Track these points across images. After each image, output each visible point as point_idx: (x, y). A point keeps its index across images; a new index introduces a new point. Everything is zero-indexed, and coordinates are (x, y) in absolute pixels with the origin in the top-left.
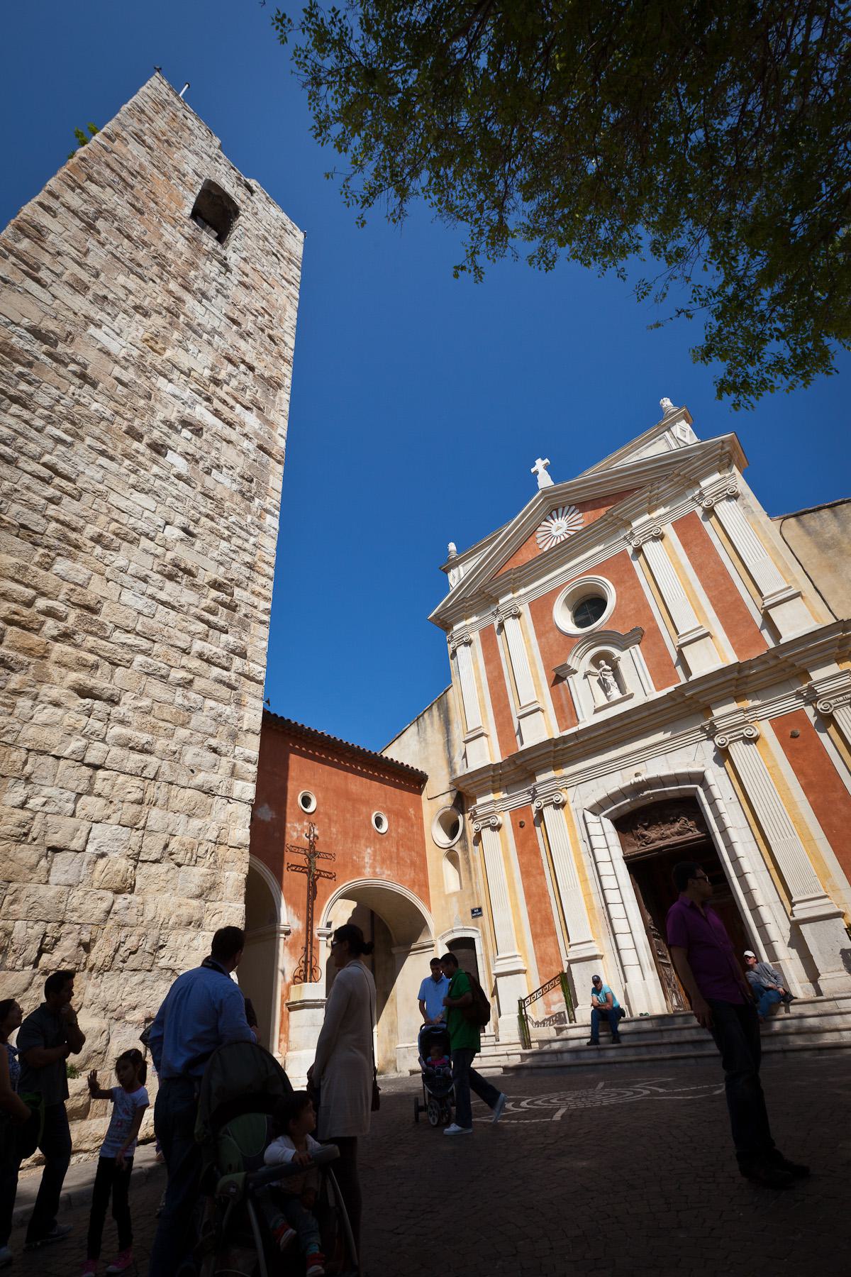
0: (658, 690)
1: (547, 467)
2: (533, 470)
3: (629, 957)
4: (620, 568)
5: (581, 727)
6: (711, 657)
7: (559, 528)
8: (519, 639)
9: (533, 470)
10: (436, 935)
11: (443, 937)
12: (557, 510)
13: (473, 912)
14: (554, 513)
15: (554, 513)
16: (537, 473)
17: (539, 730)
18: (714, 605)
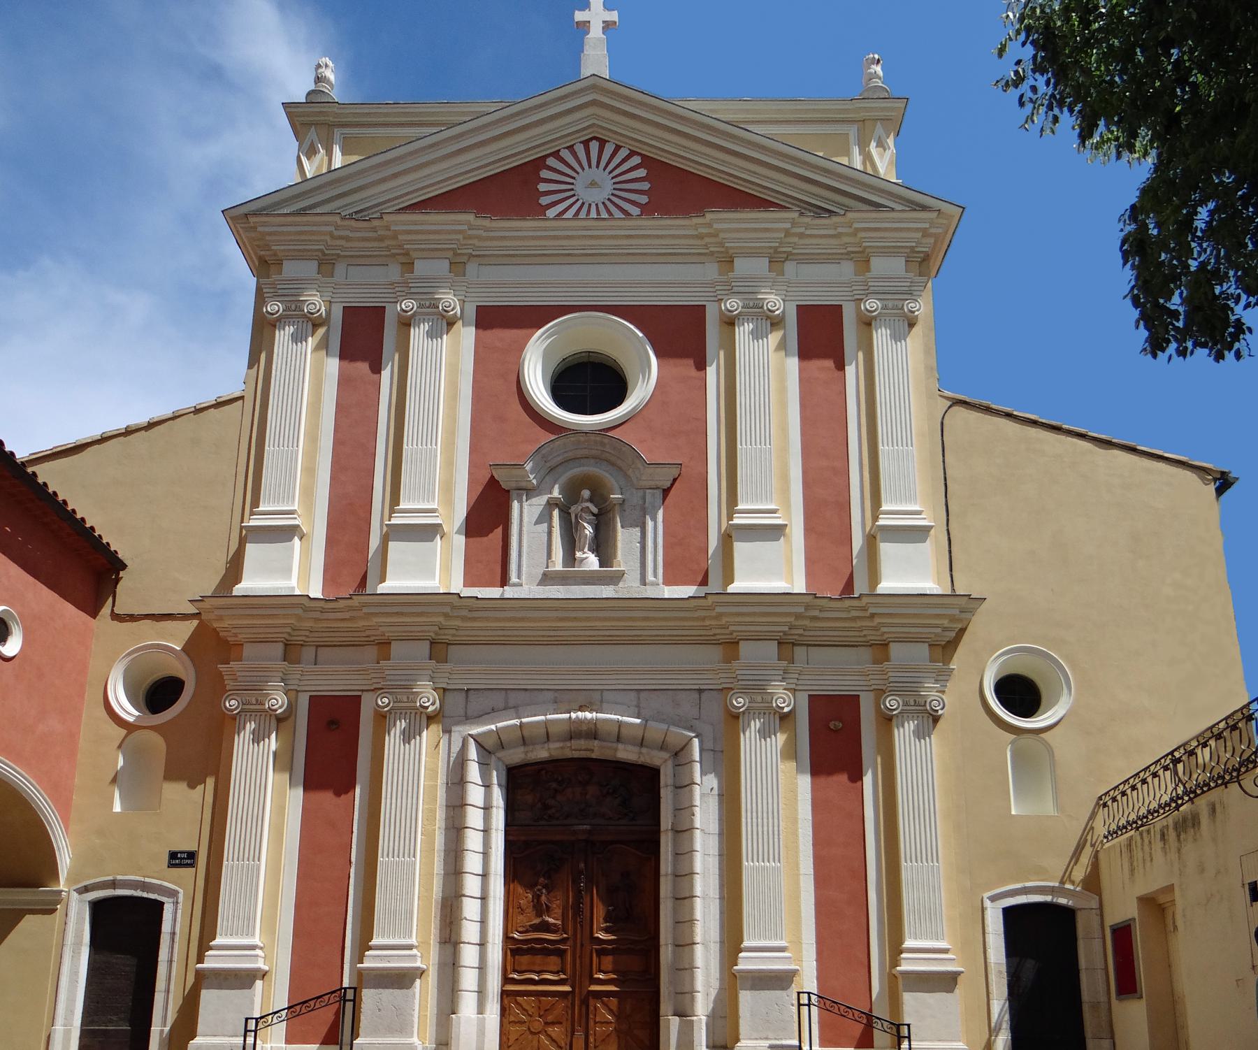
0: (668, 582)
1: (607, 26)
2: (579, 16)
3: (469, 979)
4: (681, 334)
5: (509, 592)
6: (772, 571)
7: (593, 184)
8: (440, 369)
9: (579, 16)
10: (69, 880)
11: (86, 889)
12: (603, 143)
13: (173, 855)
14: (594, 146)
15: (594, 146)
16: (584, 26)
17: (428, 570)
18: (807, 485)
